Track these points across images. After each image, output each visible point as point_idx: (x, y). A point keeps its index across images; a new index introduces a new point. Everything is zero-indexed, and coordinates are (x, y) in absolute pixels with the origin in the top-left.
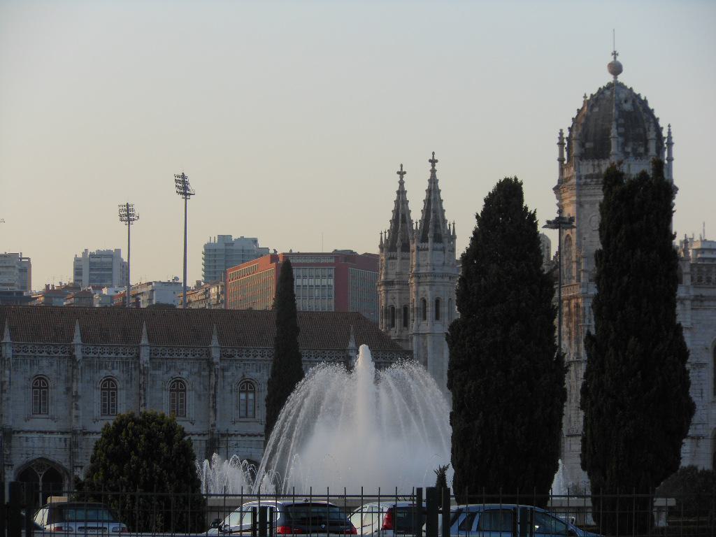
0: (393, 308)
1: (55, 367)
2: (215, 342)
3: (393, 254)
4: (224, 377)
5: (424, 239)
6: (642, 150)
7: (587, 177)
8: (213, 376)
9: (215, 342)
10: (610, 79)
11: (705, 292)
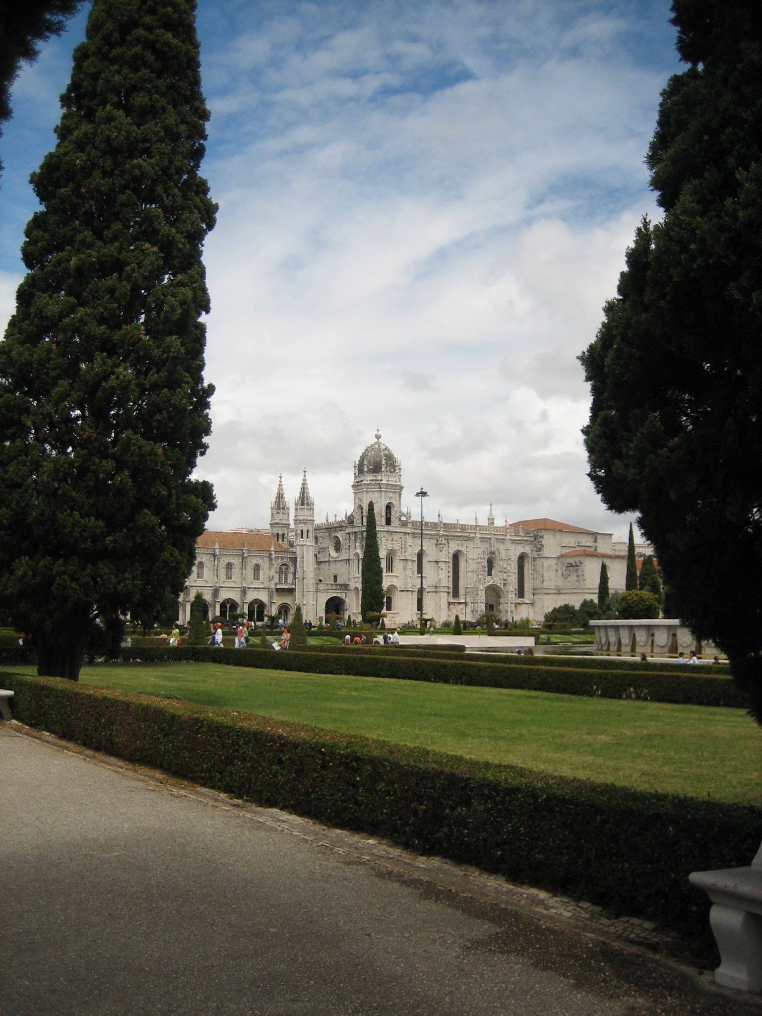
0: (278, 534)
2: (217, 546)
3: (279, 511)
5: (303, 504)
6: (392, 470)
7: (371, 480)
8: (216, 560)
9: (217, 546)
10: (376, 440)
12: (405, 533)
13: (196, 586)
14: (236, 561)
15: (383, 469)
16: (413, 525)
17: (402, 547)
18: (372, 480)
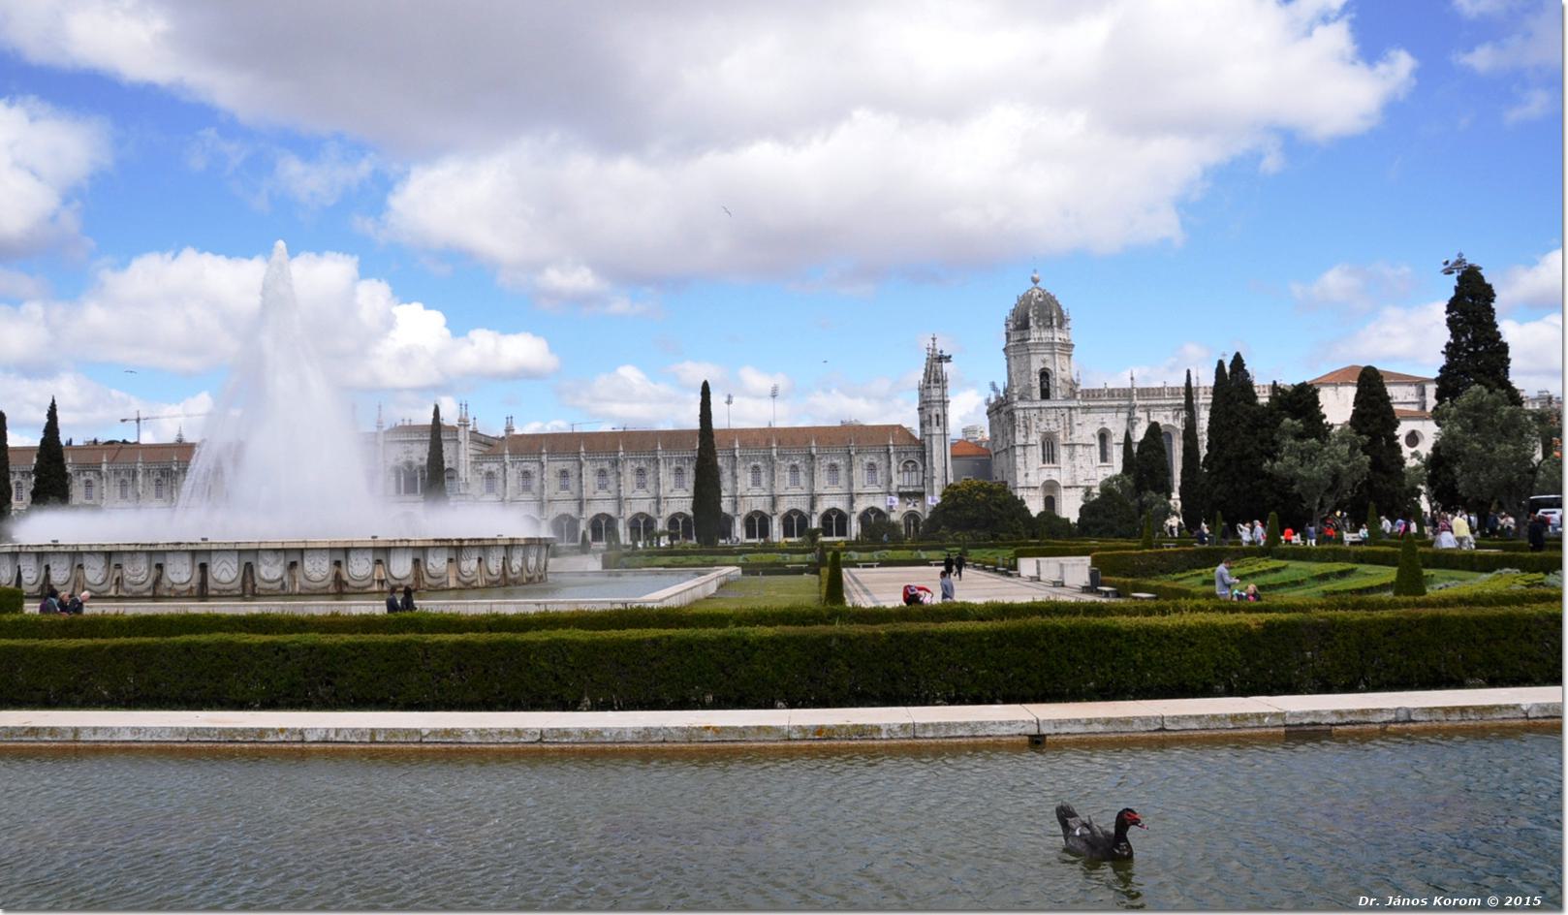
1: (725, 461)
2: (814, 444)
4: (820, 463)
6: (1049, 323)
9: (814, 444)
10: (1033, 285)
11: (1091, 404)
12: (1070, 408)
13: (789, 495)
14: (840, 462)
15: (1031, 323)
16: (1083, 396)
17: (1065, 428)
18: (1019, 341)
